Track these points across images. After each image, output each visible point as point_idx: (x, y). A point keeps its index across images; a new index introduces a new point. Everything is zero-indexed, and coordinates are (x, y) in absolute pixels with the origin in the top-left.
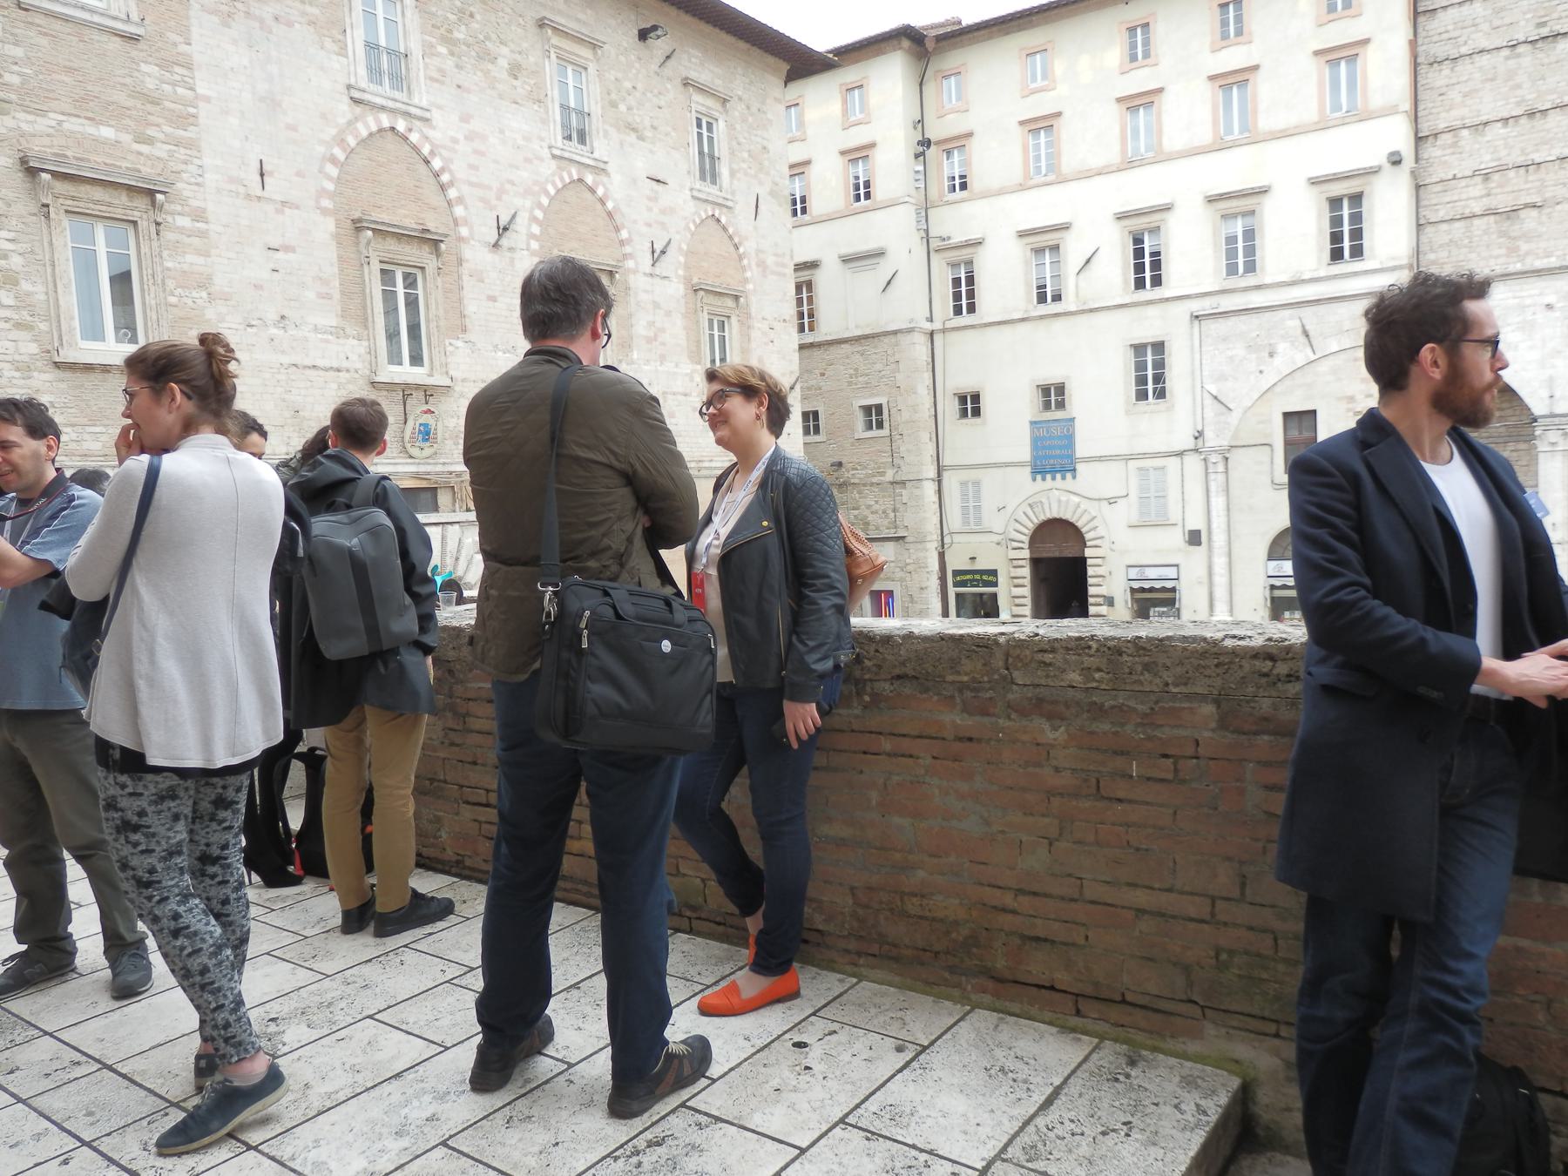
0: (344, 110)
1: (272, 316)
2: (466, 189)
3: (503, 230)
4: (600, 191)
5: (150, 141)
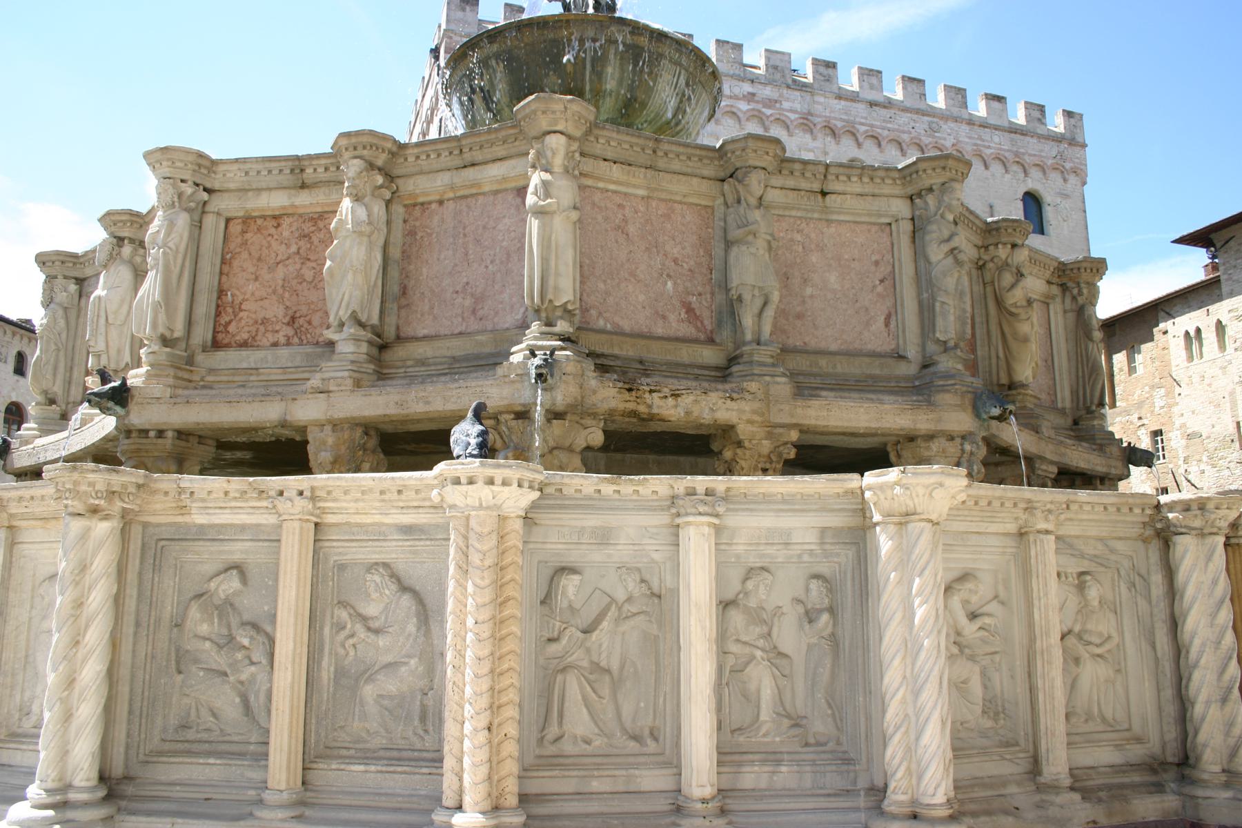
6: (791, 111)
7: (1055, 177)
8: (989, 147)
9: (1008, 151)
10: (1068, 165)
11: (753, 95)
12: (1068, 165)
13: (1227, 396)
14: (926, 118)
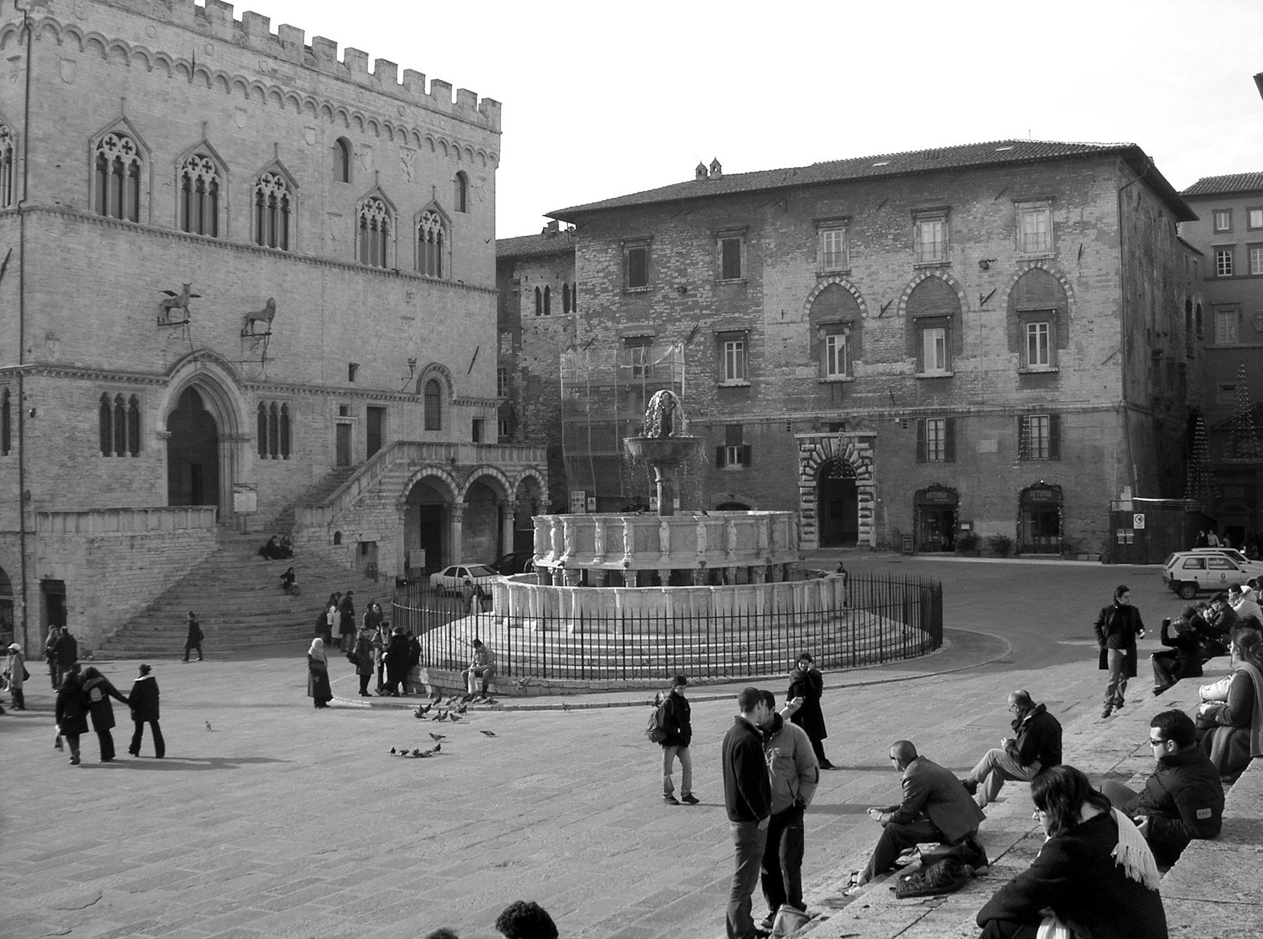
0: (813, 283)
1: (784, 362)
2: (866, 298)
3: (883, 310)
6: (302, 89)
7: (478, 159)
8: (437, 132)
9: (449, 136)
10: (488, 151)
11: (275, 71)
12: (488, 151)
14: (397, 102)
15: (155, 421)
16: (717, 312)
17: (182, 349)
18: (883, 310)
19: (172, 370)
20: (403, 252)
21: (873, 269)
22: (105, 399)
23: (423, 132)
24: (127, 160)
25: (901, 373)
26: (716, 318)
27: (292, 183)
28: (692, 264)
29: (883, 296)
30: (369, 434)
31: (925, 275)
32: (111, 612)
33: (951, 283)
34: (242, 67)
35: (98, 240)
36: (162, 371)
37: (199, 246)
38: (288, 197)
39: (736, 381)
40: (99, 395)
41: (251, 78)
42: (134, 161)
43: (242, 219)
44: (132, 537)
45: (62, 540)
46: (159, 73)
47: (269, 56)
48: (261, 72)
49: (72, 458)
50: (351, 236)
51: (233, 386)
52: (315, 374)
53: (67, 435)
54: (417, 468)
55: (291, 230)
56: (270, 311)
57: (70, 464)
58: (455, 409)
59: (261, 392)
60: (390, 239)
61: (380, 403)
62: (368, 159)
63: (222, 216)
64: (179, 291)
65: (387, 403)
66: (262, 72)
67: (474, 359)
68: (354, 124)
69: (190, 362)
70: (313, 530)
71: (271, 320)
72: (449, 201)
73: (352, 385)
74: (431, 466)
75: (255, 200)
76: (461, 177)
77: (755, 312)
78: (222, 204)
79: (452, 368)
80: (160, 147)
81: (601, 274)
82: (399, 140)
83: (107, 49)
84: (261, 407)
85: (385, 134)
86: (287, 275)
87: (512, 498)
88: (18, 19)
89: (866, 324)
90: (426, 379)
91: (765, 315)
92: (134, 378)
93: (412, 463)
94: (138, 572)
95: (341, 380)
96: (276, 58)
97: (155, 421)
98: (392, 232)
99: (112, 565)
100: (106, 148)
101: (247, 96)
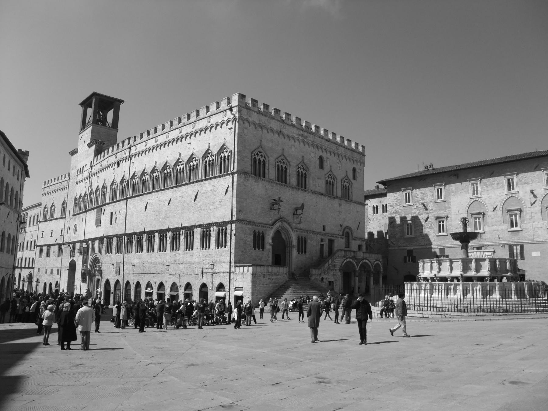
0: (469, 200)
2: (488, 205)
3: (495, 209)
4: (517, 197)
5: (445, 211)
6: (310, 140)
8: (347, 155)
10: (362, 161)
11: (303, 135)
12: (362, 161)
13: (383, 226)
15: (269, 239)
16: (435, 211)
17: (276, 217)
18: (495, 209)
19: (273, 224)
20: (339, 192)
21: (490, 195)
22: (255, 232)
23: (343, 155)
24: (262, 159)
25: (502, 229)
26: (435, 213)
27: (307, 169)
28: (425, 196)
29: (494, 204)
30: (329, 248)
31: (509, 196)
32: (257, 298)
33: (519, 198)
34: (293, 133)
35: (254, 183)
36: (271, 224)
37: (281, 186)
38: (306, 173)
39: (442, 234)
40: (253, 231)
41: (296, 137)
42: (264, 160)
43: (293, 179)
44: (264, 274)
45: (242, 274)
46: (270, 133)
47: (301, 130)
48: (299, 135)
49: (245, 249)
50: (324, 185)
51: (291, 230)
52: (314, 227)
53: (244, 242)
54: (345, 258)
55: (307, 183)
56: (302, 207)
57: (245, 251)
58: (354, 241)
59: (298, 232)
60: (335, 187)
61: (332, 238)
62: (328, 162)
63: (288, 178)
64: (277, 198)
65: (335, 238)
66: (299, 135)
67: (359, 226)
68: (324, 151)
69: (279, 222)
70: (315, 276)
71: (303, 210)
72: (351, 176)
73: (324, 232)
74: (349, 258)
75: (297, 173)
76: (354, 170)
77: (449, 211)
78: (288, 174)
79: (353, 228)
80: (271, 156)
81: (396, 200)
82: (337, 157)
83: (257, 126)
84: (298, 237)
85: (333, 155)
86: (306, 197)
87: (372, 270)
88: (232, 116)
89: (488, 213)
90: (345, 232)
91: (452, 212)
92: (262, 225)
93: (344, 257)
94: (265, 286)
95: (321, 230)
96: (303, 131)
97: (269, 239)
98: (335, 185)
99: (258, 283)
100: (256, 156)
101: (295, 142)
